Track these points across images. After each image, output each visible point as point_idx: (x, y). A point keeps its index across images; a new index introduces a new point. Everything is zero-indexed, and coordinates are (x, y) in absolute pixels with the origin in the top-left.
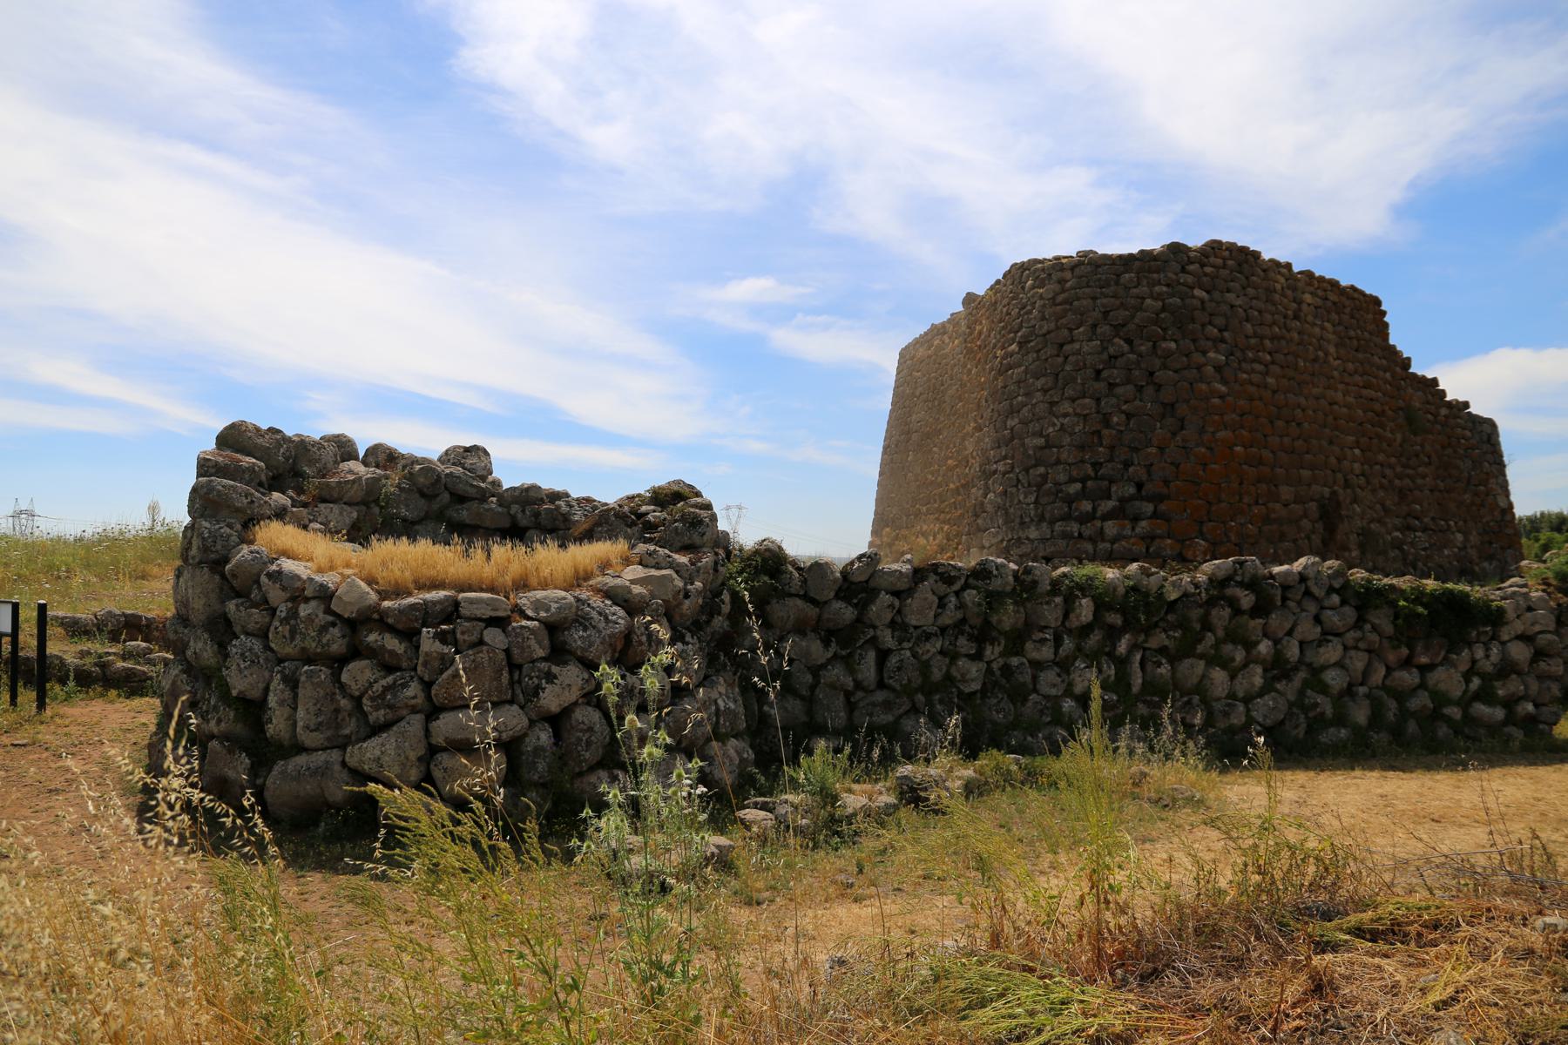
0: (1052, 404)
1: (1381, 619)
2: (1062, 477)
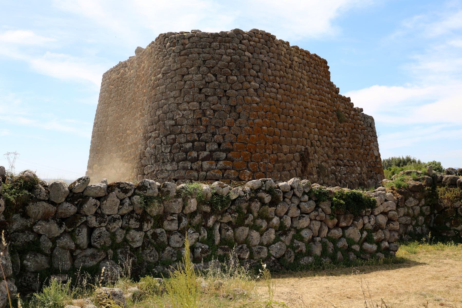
0: (178, 104)
1: (326, 206)
2: (183, 140)
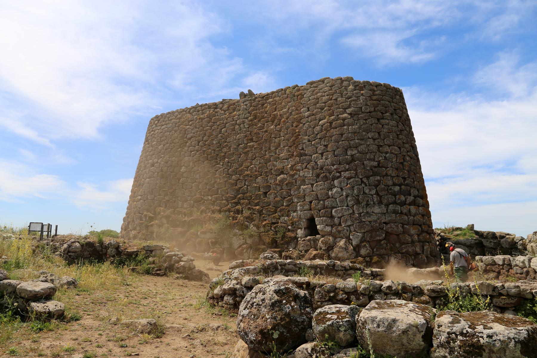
0: (379, 146)
2: (390, 183)
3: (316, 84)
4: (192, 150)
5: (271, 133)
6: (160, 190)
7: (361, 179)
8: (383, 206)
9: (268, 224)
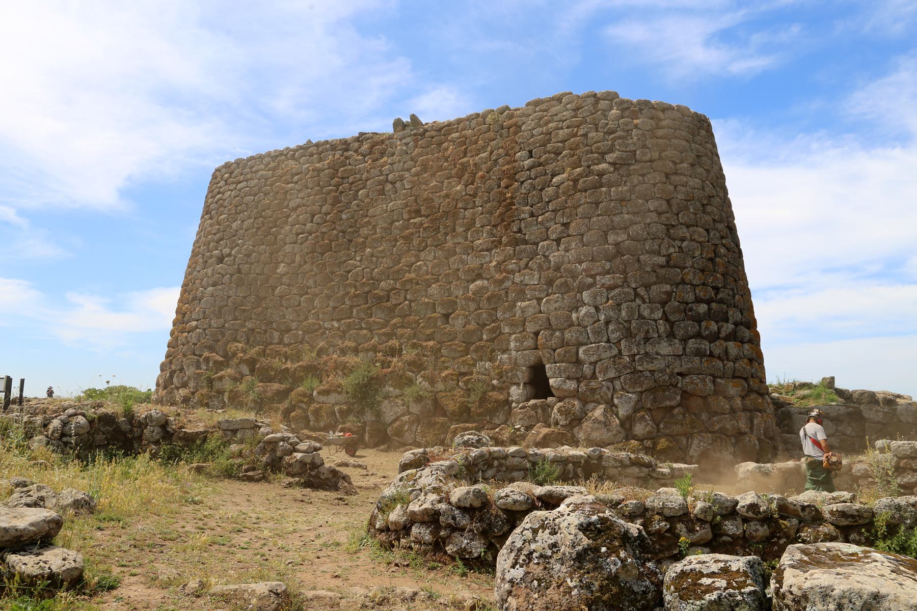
0: (669, 227)
2: (691, 297)
3: (546, 104)
4: (299, 231)
5: (457, 200)
6: (236, 308)
7: (635, 289)
8: (677, 341)
9: (452, 375)
